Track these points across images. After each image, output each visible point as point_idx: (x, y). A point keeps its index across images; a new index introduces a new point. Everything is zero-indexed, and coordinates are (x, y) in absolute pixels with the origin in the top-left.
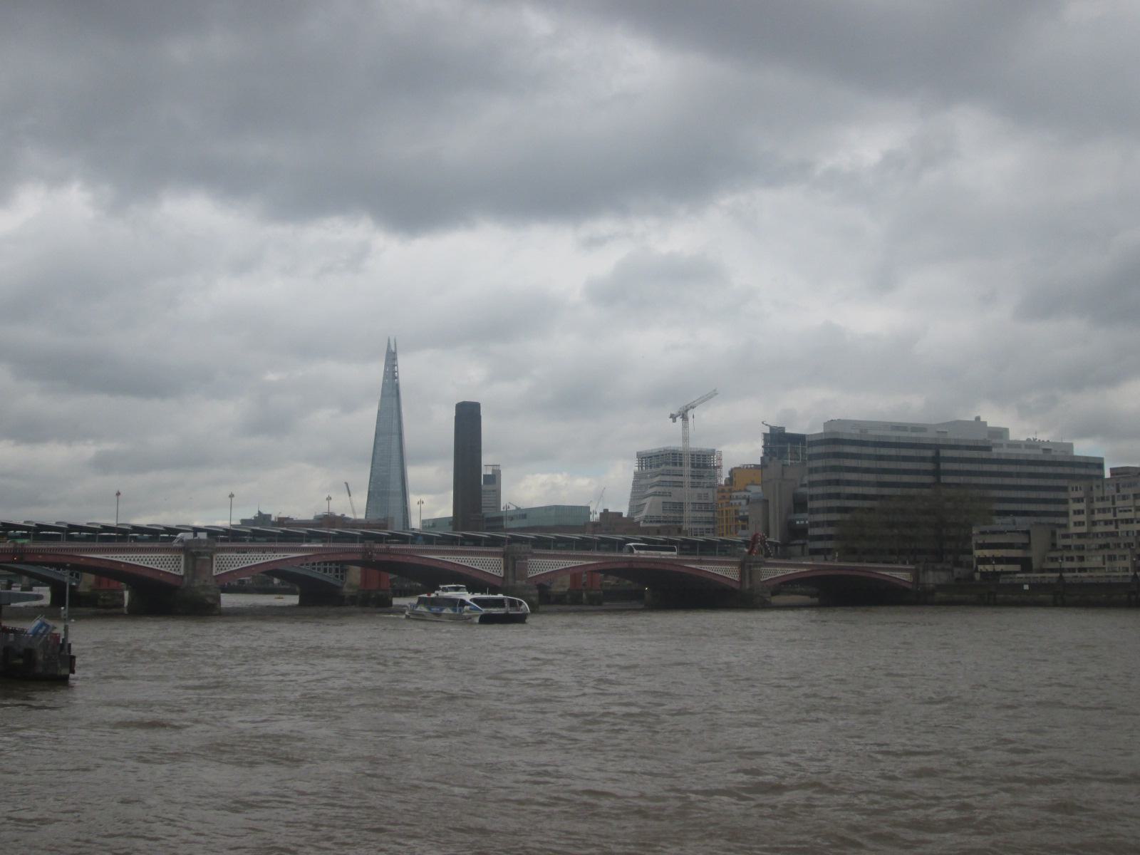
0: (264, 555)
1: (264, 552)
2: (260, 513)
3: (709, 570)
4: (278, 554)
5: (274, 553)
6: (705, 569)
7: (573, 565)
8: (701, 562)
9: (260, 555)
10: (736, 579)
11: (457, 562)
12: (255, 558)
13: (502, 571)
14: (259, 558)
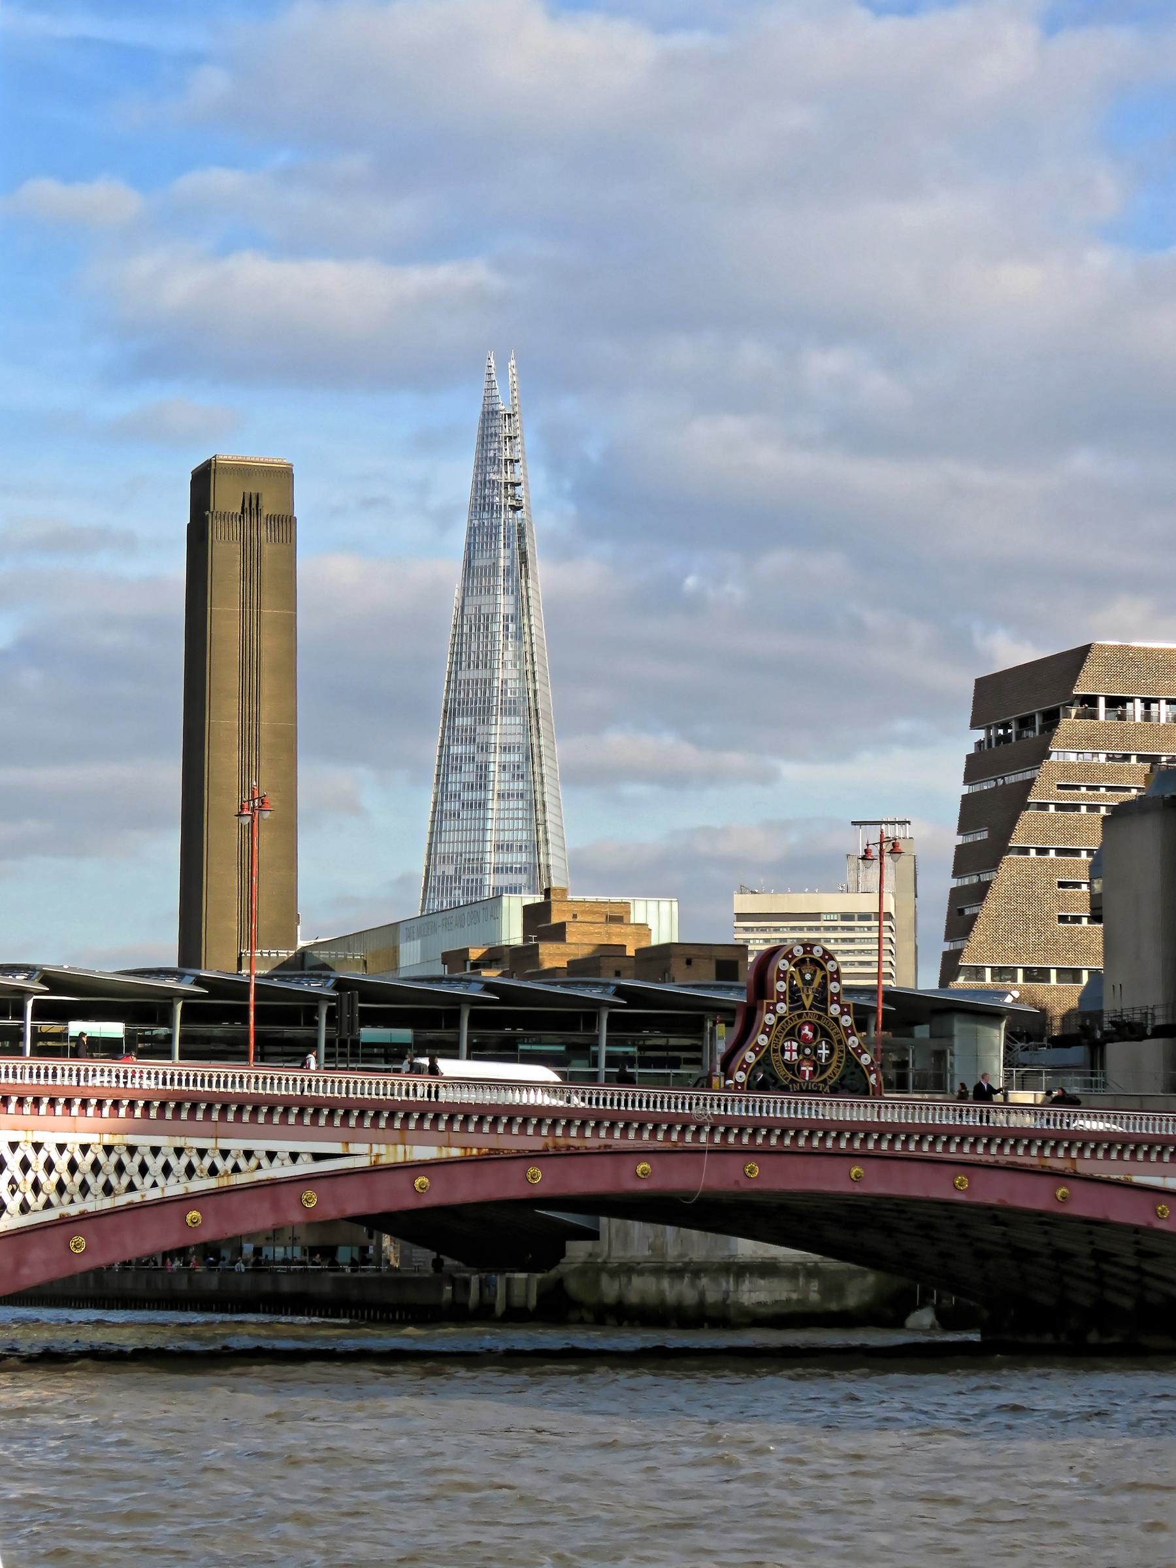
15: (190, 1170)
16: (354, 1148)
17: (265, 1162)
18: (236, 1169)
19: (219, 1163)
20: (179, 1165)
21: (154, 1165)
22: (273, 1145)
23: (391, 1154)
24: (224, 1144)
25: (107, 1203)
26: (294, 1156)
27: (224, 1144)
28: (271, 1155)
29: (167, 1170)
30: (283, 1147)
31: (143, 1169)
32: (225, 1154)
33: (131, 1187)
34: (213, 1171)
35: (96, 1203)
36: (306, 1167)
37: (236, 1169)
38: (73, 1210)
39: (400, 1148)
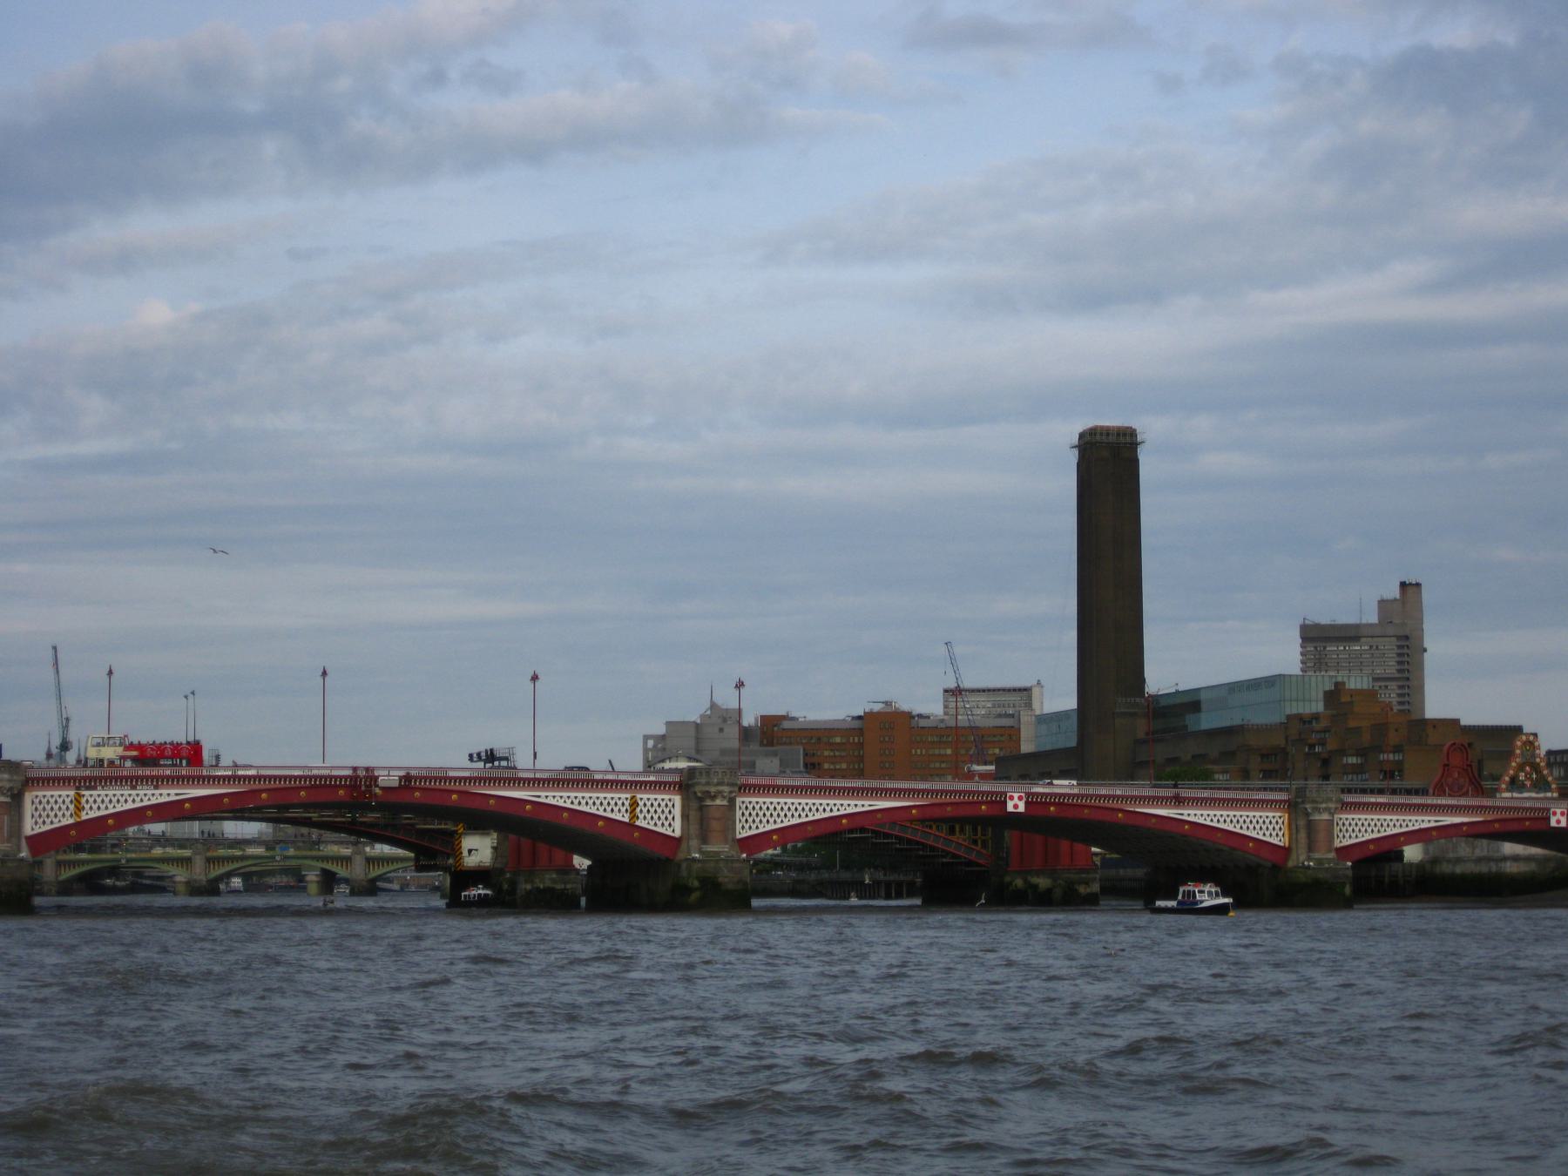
0: (134, 792)
1: (134, 788)
2: (713, 706)
3: (1201, 821)
4: (165, 792)
5: (156, 787)
6: (1191, 819)
7: (850, 810)
8: (1179, 801)
9: (126, 793)
11: (568, 805)
12: (114, 800)
13: (677, 825)
14: (122, 799)
15: (1401, 826)
20: (1398, 824)
26: (1429, 821)
28: (1423, 821)
29: (1394, 825)
30: (1426, 818)
36: (1433, 824)
38: (1370, 838)
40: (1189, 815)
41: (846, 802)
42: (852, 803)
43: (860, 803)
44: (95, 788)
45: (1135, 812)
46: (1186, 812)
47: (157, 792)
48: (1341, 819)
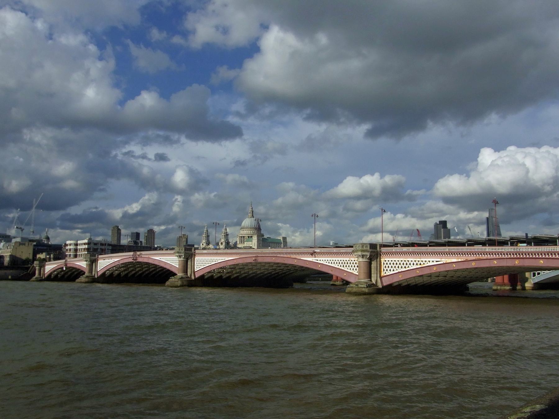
6: (321, 262)
10: (356, 273)
15: (417, 264)
16: (442, 260)
17: (428, 262)
18: (424, 264)
19: (421, 263)
20: (415, 263)
21: (412, 263)
22: (429, 260)
23: (449, 261)
24: (422, 260)
25: (405, 270)
26: (433, 261)
27: (422, 260)
28: (429, 261)
29: (413, 264)
30: (431, 260)
31: (410, 264)
32: (422, 261)
33: (408, 267)
34: (420, 264)
35: (404, 269)
36: (435, 263)
37: (424, 264)
39: (450, 259)
40: (320, 260)
41: (219, 258)
42: (220, 258)
43: (222, 258)
44: (104, 260)
45: (300, 259)
46: (319, 259)
47: (111, 260)
48: (385, 261)
